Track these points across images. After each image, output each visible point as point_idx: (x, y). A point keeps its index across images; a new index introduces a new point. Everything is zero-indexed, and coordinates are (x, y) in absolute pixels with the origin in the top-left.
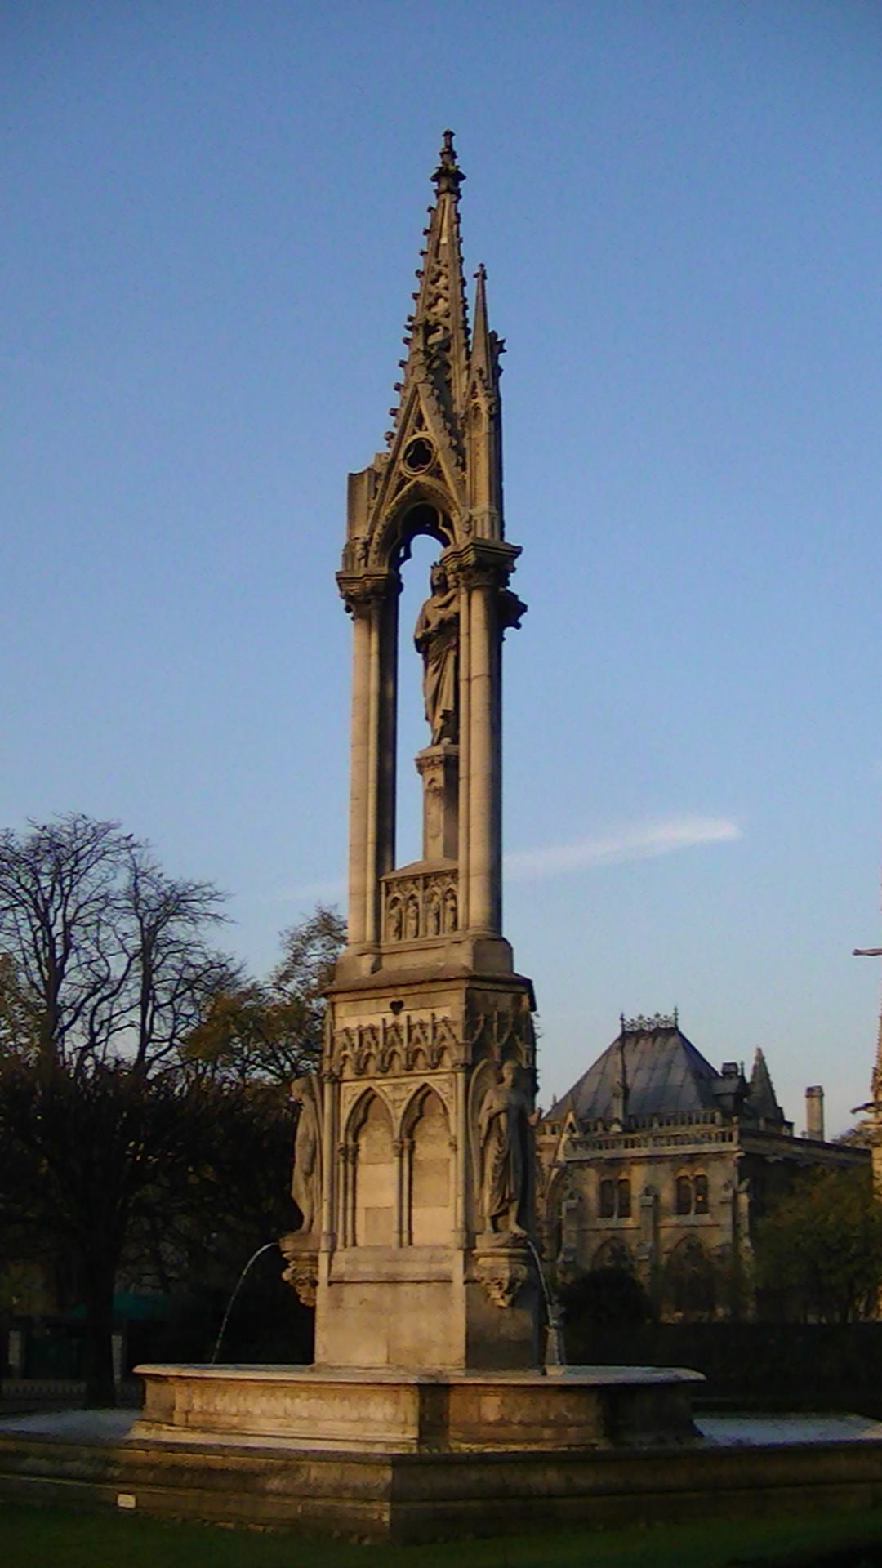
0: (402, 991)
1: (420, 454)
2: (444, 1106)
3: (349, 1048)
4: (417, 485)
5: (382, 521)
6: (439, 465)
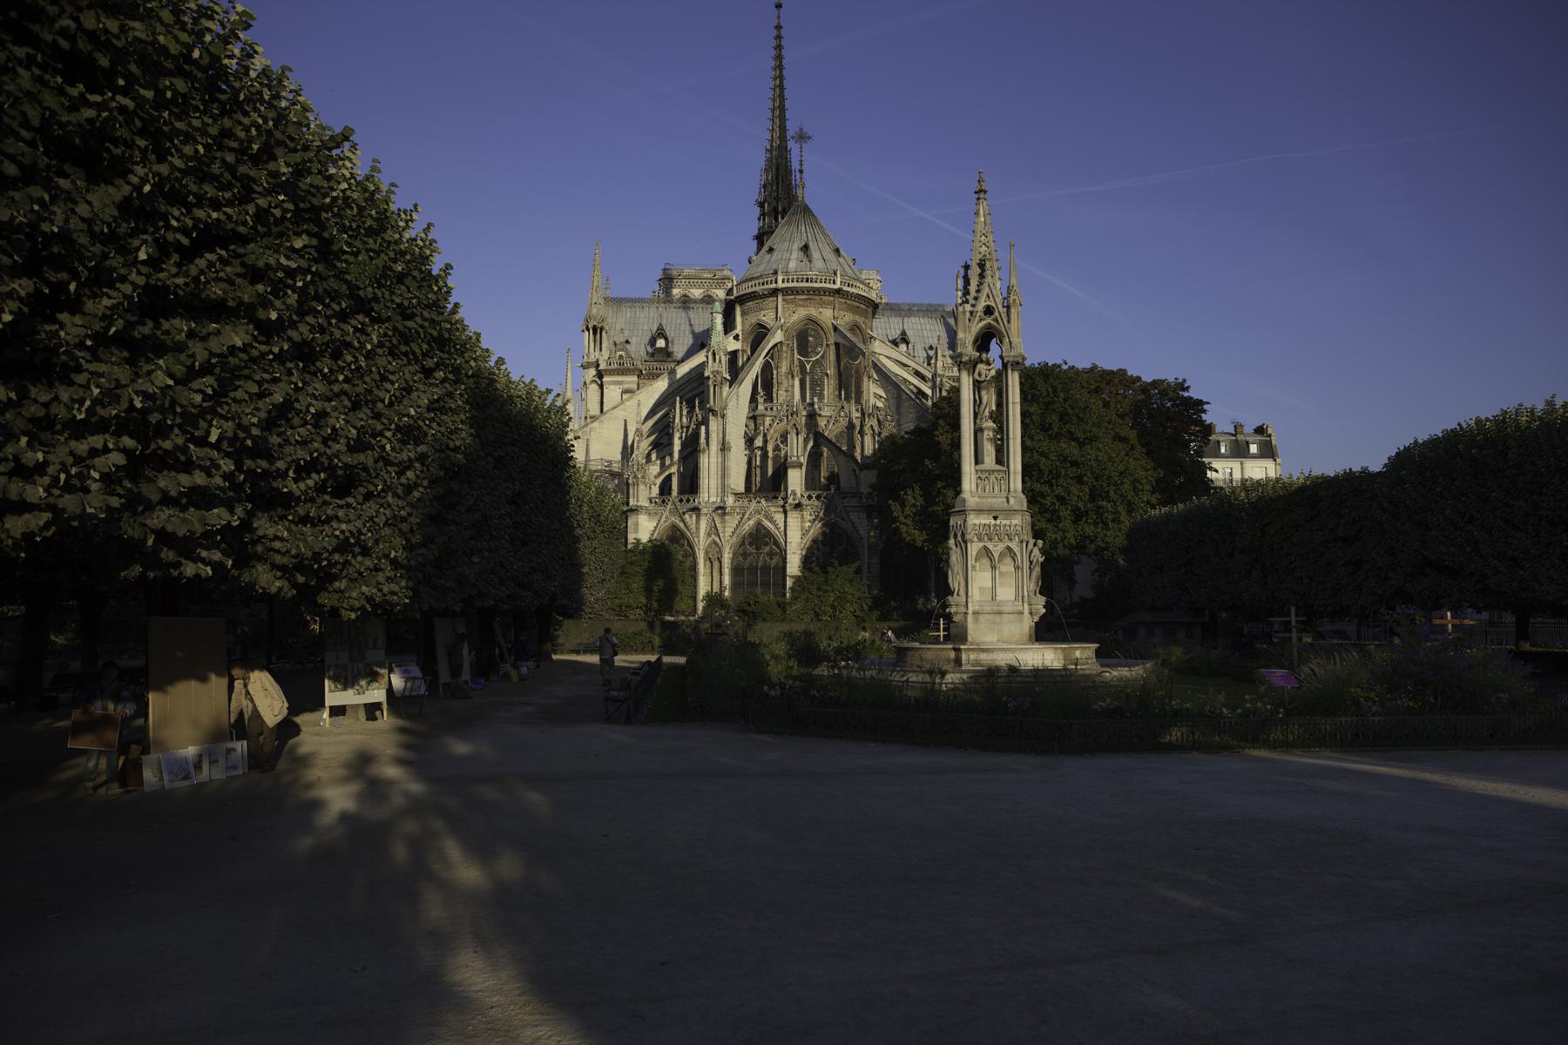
0: (998, 512)
4: (989, 324)
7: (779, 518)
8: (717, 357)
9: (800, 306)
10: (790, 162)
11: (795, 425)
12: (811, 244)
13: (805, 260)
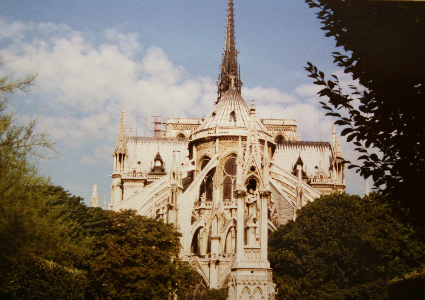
1: (253, 169)
2: (261, 290)
5: (245, 180)
7: (205, 268)
8: (176, 176)
9: (228, 146)
10: (237, 61)
11: (216, 215)
12: (236, 112)
13: (233, 120)
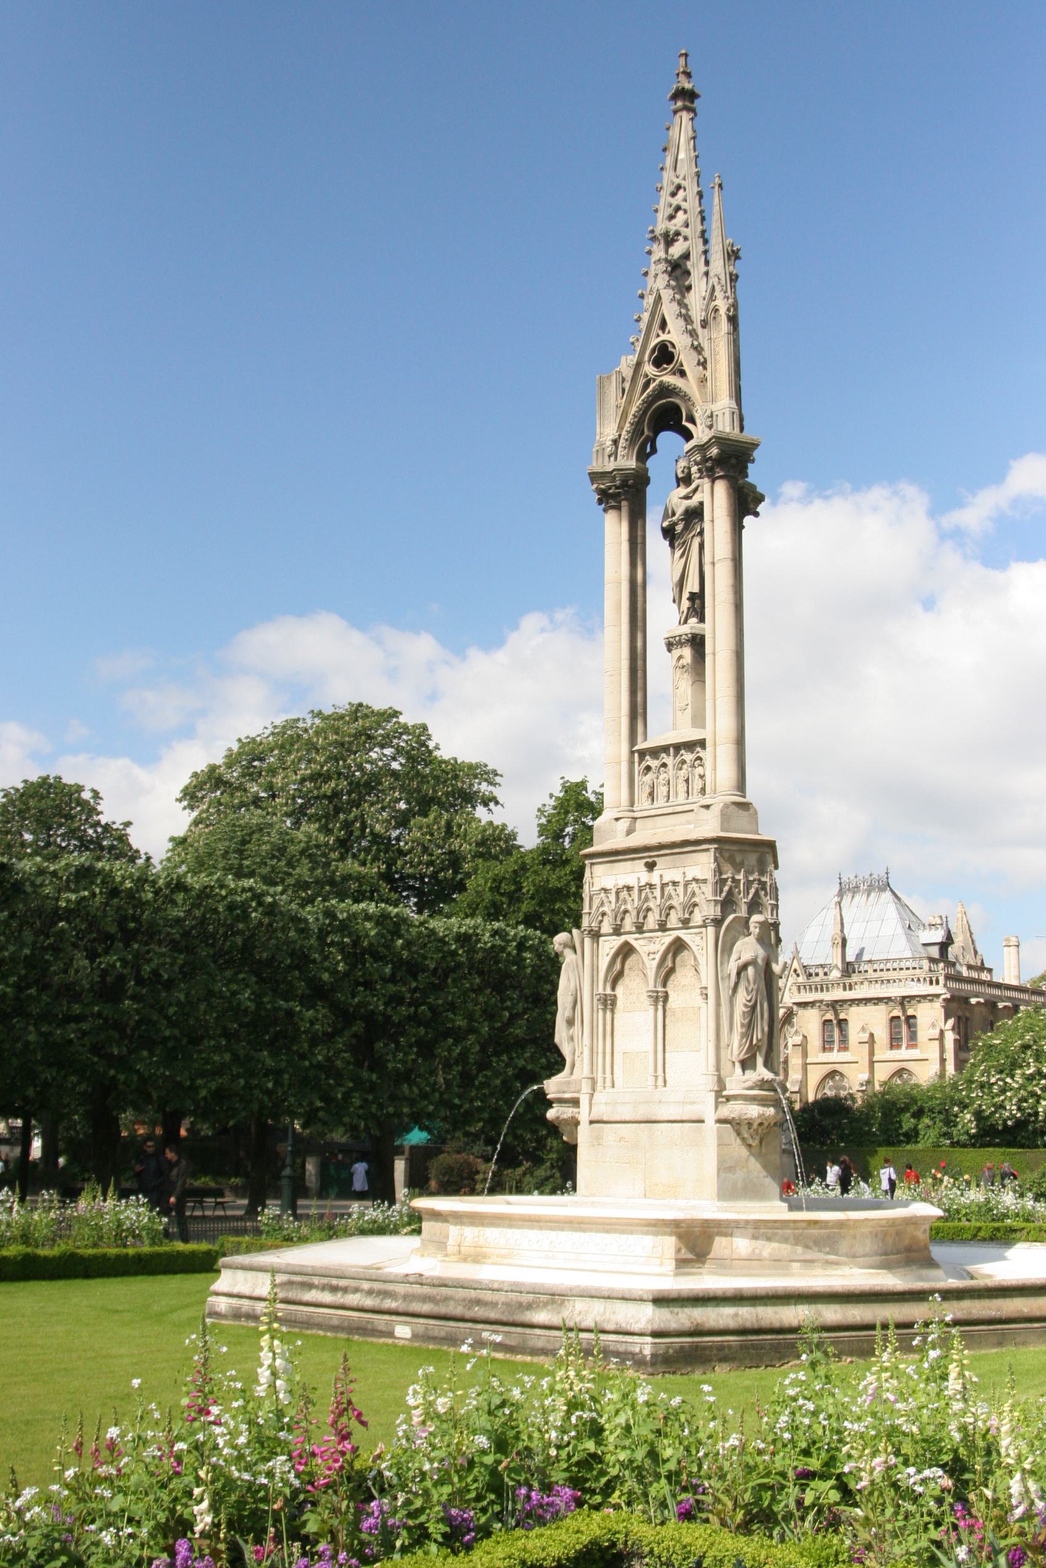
1: (664, 356)
2: (695, 959)
3: (606, 904)
5: (630, 417)
6: (682, 365)
